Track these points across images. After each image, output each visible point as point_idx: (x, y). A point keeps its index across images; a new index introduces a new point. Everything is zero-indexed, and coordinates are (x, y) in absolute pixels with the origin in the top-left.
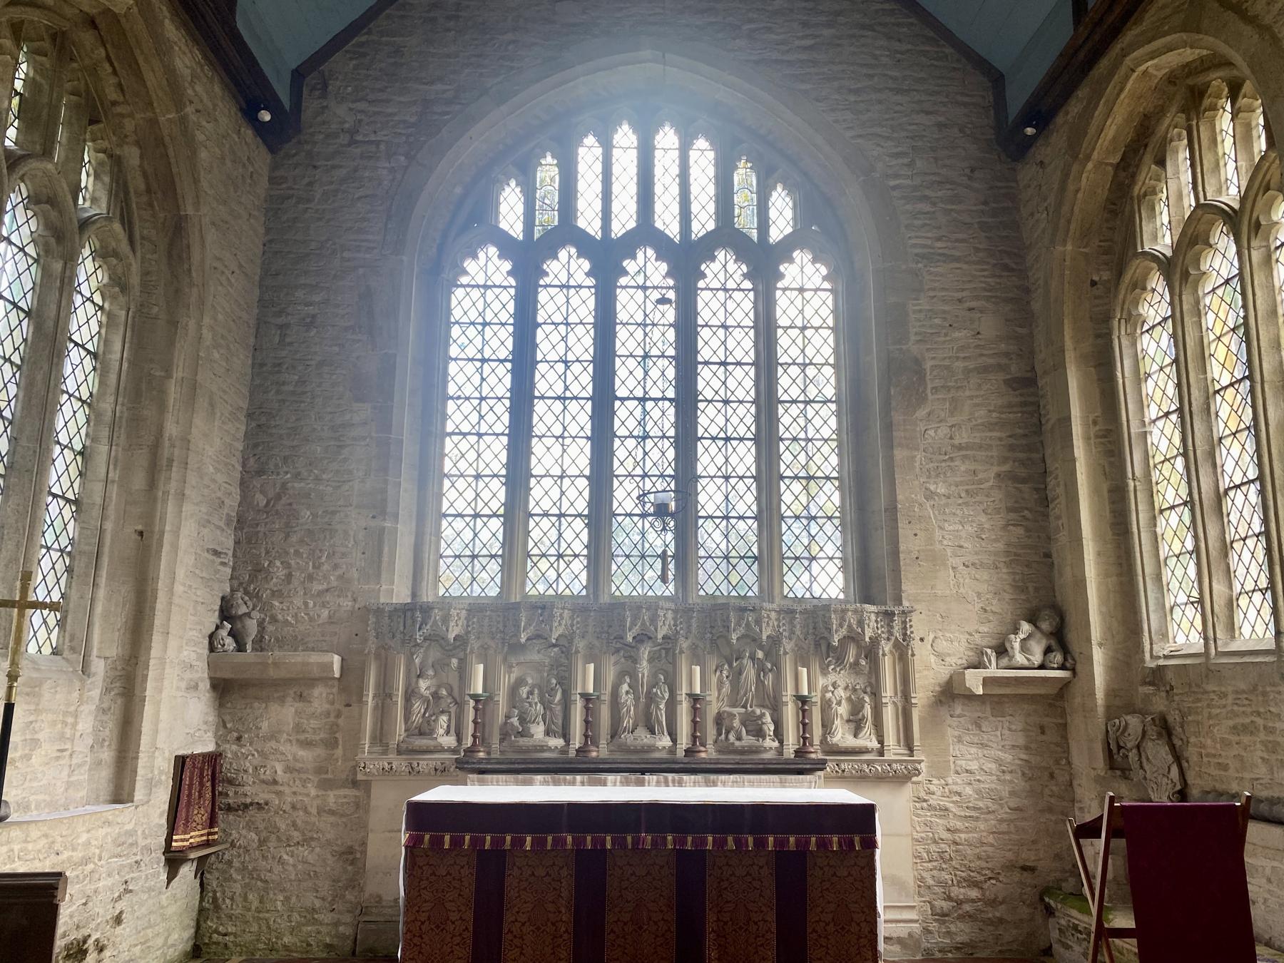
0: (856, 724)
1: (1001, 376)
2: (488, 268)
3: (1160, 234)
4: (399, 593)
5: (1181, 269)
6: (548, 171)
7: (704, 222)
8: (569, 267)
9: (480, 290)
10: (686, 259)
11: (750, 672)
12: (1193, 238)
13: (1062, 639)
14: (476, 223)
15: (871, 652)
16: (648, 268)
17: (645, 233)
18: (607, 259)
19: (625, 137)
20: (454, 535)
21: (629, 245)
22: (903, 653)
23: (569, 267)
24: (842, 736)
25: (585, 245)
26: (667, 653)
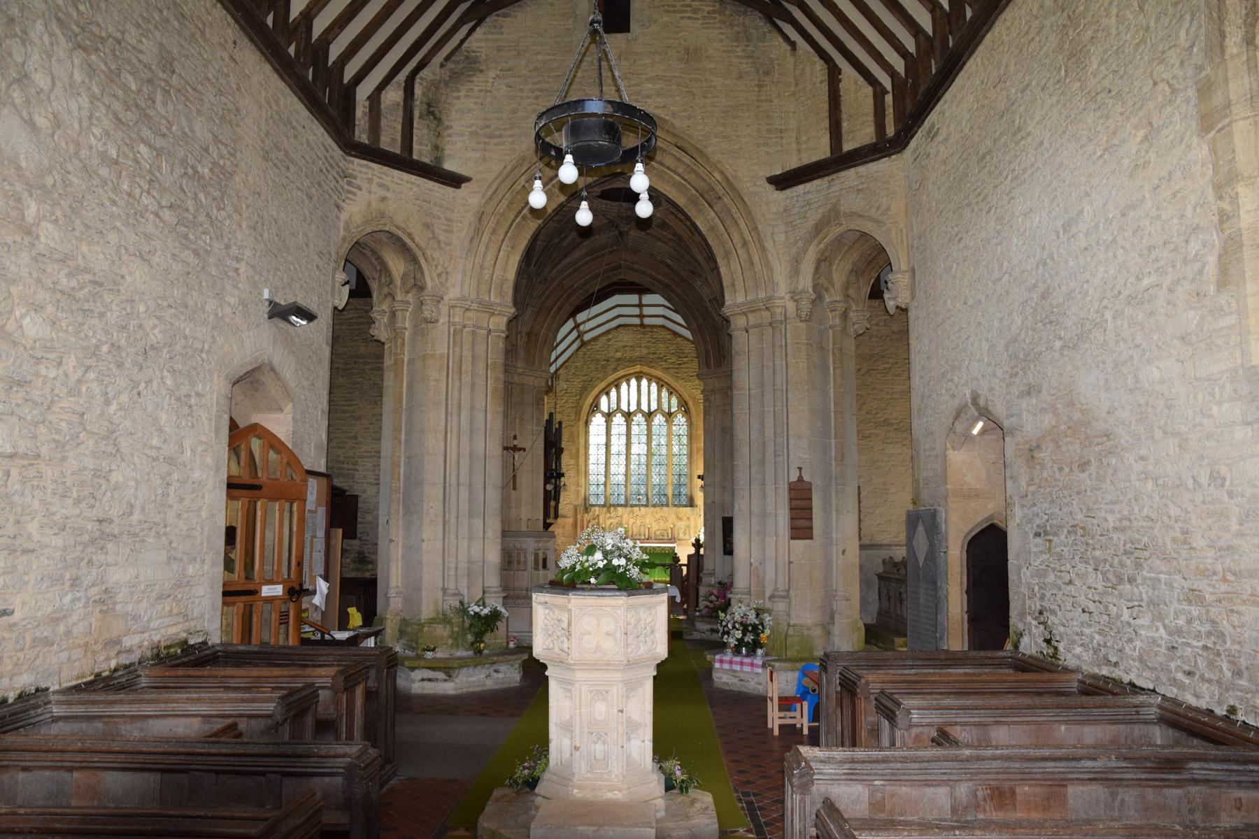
2: (598, 421)
6: (613, 393)
8: (618, 419)
10: (649, 416)
14: (595, 407)
16: (639, 418)
18: (628, 416)
19: (633, 382)
21: (635, 413)
23: (618, 419)
24: (681, 536)
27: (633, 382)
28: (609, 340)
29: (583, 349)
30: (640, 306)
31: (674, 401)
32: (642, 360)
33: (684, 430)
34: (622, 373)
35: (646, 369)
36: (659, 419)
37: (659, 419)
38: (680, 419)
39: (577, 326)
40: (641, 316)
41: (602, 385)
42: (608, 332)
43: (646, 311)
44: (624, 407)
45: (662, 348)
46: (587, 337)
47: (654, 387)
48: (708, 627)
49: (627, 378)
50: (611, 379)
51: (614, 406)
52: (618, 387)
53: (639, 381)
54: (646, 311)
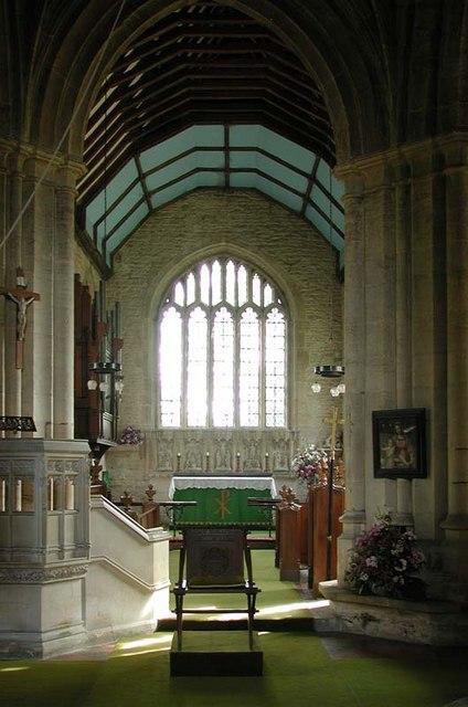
0: (282, 463)
4: (153, 428)
6: (191, 279)
7: (243, 299)
8: (198, 315)
9: (170, 321)
10: (236, 313)
11: (253, 449)
14: (167, 297)
15: (287, 444)
17: (224, 303)
20: (165, 407)
21: (218, 307)
22: (297, 444)
23: (198, 315)
25: (203, 307)
26: (230, 443)
27: (216, 266)
29: (151, 219)
30: (227, 149)
31: (269, 291)
35: (233, 248)
36: (249, 316)
37: (249, 316)
39: (142, 177)
40: (227, 170)
42: (183, 197)
43: (237, 160)
44: (205, 299)
46: (157, 200)
47: (243, 272)
48: (359, 611)
50: (188, 259)
51: (191, 299)
52: (196, 272)
54: (237, 160)
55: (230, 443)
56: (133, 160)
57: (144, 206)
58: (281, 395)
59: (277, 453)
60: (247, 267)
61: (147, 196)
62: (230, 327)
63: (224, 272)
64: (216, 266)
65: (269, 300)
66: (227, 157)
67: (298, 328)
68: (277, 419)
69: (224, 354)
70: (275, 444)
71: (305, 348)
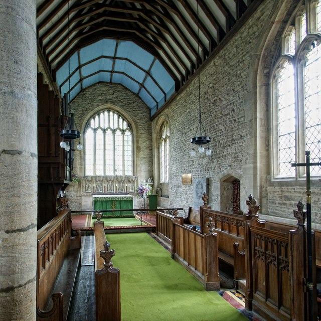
0: (132, 189)
1: (148, 149)
3: (164, 137)
5: (165, 141)
6: (97, 117)
8: (100, 132)
10: (114, 131)
12: (166, 138)
13: (153, 180)
15: (134, 182)
16: (109, 132)
17: (109, 128)
18: (104, 131)
21: (107, 129)
22: (137, 182)
23: (100, 132)
27: (106, 113)
28: (95, 89)
31: (125, 124)
32: (113, 102)
33: (130, 138)
34: (101, 107)
36: (118, 133)
37: (118, 133)
38: (128, 133)
41: (91, 113)
43: (120, 66)
44: (102, 126)
45: (120, 95)
49: (103, 110)
52: (99, 115)
53: (109, 113)
55: (113, 181)
56: (77, 52)
57: (79, 86)
58: (130, 163)
59: (130, 185)
60: (117, 114)
61: (81, 80)
62: (112, 137)
63: (109, 116)
64: (106, 113)
65: (125, 126)
66: (111, 76)
67: (137, 137)
68: (129, 173)
69: (109, 147)
70: (129, 182)
71: (140, 145)
